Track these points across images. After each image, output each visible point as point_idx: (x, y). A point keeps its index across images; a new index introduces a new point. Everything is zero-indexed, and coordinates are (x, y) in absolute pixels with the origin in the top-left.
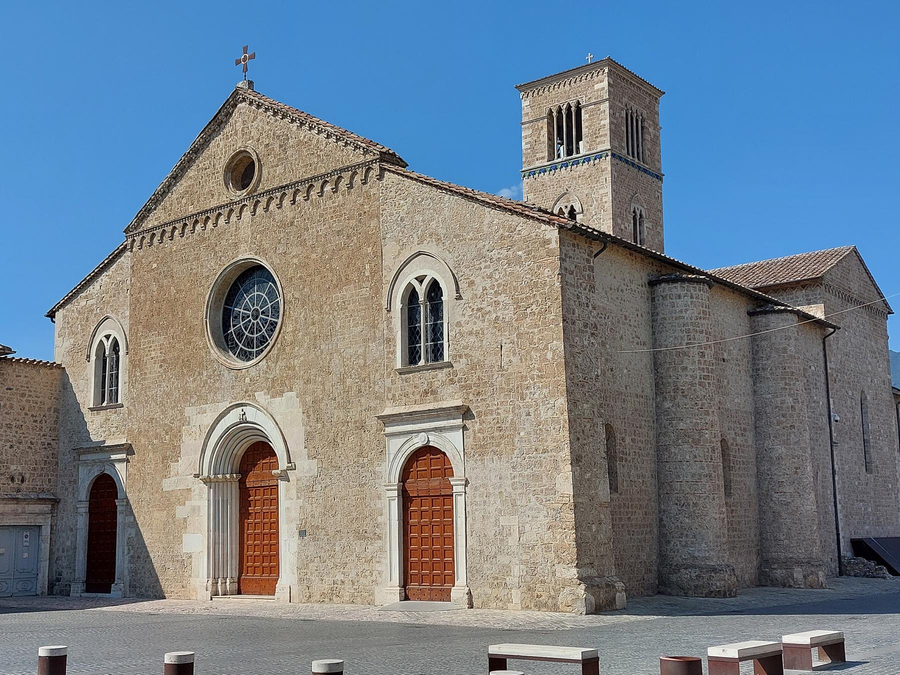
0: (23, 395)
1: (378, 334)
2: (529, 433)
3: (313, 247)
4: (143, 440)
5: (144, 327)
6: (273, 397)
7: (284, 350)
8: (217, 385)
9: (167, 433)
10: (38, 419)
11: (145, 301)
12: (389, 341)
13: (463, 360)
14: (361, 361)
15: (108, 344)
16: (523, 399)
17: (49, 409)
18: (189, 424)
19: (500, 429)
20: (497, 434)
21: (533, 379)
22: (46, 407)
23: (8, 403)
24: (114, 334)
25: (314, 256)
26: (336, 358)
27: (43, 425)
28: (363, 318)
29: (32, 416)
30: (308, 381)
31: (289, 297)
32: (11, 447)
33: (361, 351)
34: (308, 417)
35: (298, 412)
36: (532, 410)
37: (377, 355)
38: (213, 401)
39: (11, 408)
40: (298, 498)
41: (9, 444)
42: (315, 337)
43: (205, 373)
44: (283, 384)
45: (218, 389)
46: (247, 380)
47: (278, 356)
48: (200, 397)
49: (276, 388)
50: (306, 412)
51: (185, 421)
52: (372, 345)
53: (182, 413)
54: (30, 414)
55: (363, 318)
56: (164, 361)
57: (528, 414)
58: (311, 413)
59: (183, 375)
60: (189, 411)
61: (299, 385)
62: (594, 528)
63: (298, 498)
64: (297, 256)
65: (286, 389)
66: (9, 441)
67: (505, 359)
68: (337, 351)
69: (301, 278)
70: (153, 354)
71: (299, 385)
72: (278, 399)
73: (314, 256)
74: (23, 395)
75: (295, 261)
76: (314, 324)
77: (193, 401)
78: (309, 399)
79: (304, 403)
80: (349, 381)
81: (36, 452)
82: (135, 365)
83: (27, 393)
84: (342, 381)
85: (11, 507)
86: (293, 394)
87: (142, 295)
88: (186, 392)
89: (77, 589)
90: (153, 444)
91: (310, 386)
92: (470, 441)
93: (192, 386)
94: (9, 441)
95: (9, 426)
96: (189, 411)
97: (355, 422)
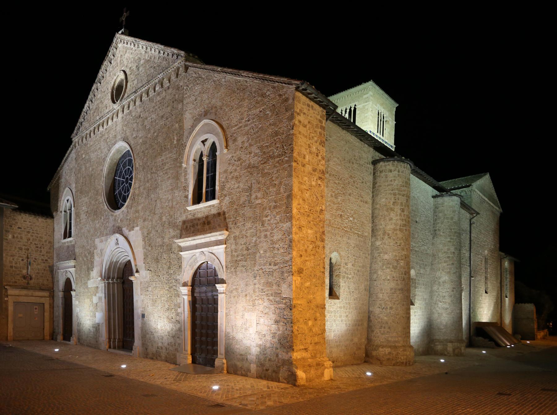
0: (28, 232)
2: (265, 251)
10: (39, 246)
12: (185, 189)
13: (227, 198)
14: (170, 204)
16: (263, 225)
17: (46, 241)
19: (248, 249)
20: (245, 252)
22: (44, 240)
23: (19, 236)
27: (42, 249)
29: (35, 244)
30: (144, 221)
32: (23, 260)
33: (170, 198)
35: (140, 239)
36: (268, 233)
39: (21, 238)
41: (21, 259)
46: (119, 221)
54: (33, 243)
56: (87, 212)
57: (266, 236)
61: (140, 222)
62: (310, 323)
66: (20, 257)
71: (140, 222)
72: (132, 232)
74: (28, 232)
79: (143, 233)
80: (164, 218)
81: (38, 264)
82: (78, 215)
83: (31, 231)
84: (161, 218)
85: (24, 292)
89: (60, 338)
91: (146, 223)
94: (20, 257)
95: (21, 249)
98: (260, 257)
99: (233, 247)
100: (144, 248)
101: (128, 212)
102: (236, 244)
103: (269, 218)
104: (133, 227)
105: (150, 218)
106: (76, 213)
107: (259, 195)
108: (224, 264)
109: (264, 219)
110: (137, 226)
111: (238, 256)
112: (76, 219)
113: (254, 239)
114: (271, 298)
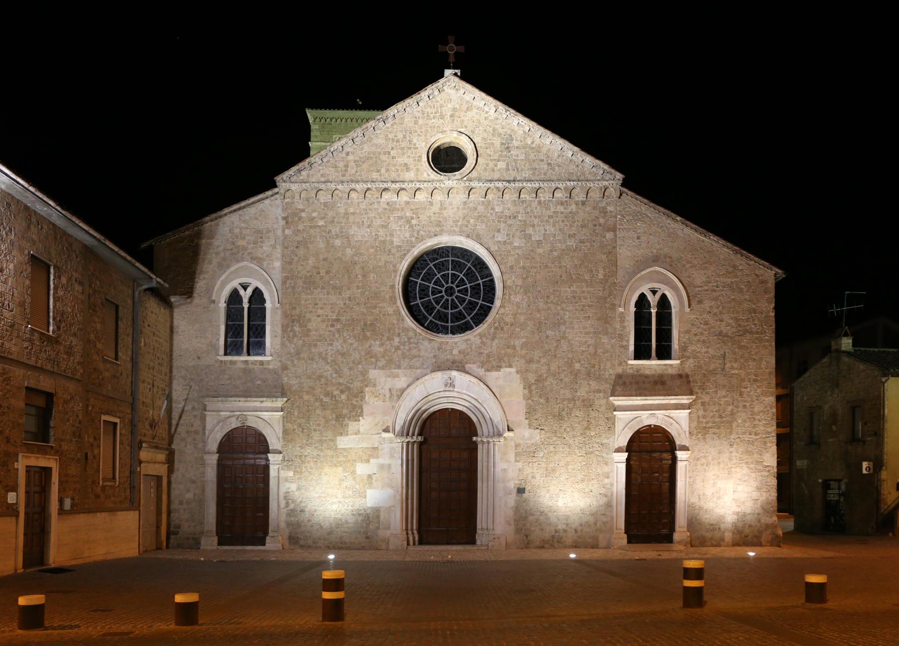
1: (610, 330)
3: (539, 243)
4: (306, 397)
5: (305, 283)
6: (488, 370)
7: (502, 329)
8: (414, 352)
9: (342, 392)
11: (306, 259)
13: (691, 360)
14: (591, 349)
15: (245, 295)
18: (375, 385)
19: (721, 417)
20: (717, 420)
21: (749, 381)
24: (255, 283)
25: (540, 251)
26: (564, 346)
28: (596, 314)
30: (530, 361)
31: (509, 283)
34: (530, 392)
36: (748, 404)
37: (609, 347)
38: (411, 367)
40: (516, 461)
42: (540, 323)
43: (397, 340)
44: (500, 359)
45: (415, 357)
47: (495, 334)
48: (390, 361)
49: (494, 363)
50: (528, 386)
51: (366, 382)
52: (605, 339)
53: (364, 373)
55: (596, 314)
56: (338, 320)
57: (745, 406)
58: (534, 387)
59: (366, 338)
60: (373, 373)
63: (516, 461)
64: (519, 247)
65: (504, 364)
67: (728, 365)
68: (564, 338)
69: (524, 268)
70: (320, 312)
72: (494, 374)
73: (540, 251)
75: (517, 251)
76: (539, 311)
77: (380, 364)
78: (532, 378)
79: (525, 380)
84: (570, 364)
86: (513, 370)
87: (301, 252)
88: (369, 354)
90: (321, 400)
91: (534, 366)
92: (695, 424)
93: (377, 349)
96: (373, 373)
97: (583, 401)
98: (738, 426)
99: (701, 413)
100: (526, 398)
101: (482, 343)
102: (704, 411)
103: (748, 390)
104: (500, 367)
105: (543, 361)
106: (285, 315)
107: (735, 365)
108: (687, 429)
109: (743, 390)
110: (510, 366)
111: (707, 423)
112: (284, 328)
113: (730, 408)
114: (752, 466)
